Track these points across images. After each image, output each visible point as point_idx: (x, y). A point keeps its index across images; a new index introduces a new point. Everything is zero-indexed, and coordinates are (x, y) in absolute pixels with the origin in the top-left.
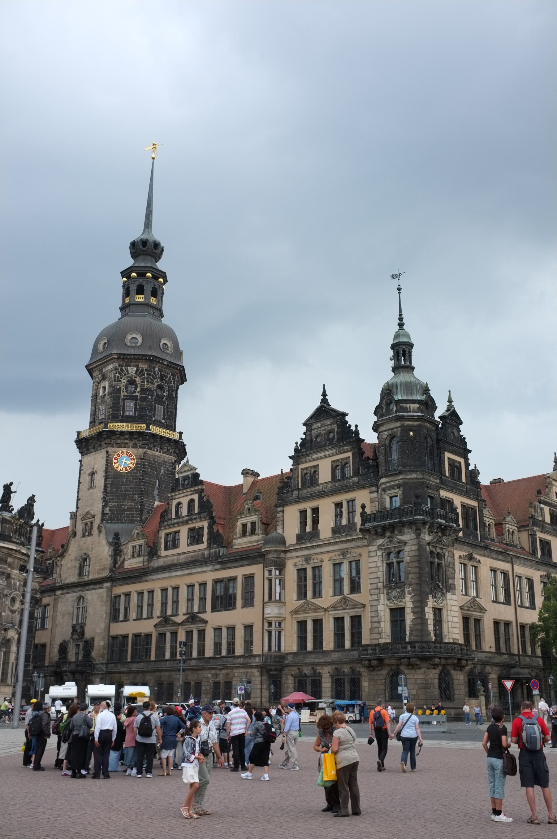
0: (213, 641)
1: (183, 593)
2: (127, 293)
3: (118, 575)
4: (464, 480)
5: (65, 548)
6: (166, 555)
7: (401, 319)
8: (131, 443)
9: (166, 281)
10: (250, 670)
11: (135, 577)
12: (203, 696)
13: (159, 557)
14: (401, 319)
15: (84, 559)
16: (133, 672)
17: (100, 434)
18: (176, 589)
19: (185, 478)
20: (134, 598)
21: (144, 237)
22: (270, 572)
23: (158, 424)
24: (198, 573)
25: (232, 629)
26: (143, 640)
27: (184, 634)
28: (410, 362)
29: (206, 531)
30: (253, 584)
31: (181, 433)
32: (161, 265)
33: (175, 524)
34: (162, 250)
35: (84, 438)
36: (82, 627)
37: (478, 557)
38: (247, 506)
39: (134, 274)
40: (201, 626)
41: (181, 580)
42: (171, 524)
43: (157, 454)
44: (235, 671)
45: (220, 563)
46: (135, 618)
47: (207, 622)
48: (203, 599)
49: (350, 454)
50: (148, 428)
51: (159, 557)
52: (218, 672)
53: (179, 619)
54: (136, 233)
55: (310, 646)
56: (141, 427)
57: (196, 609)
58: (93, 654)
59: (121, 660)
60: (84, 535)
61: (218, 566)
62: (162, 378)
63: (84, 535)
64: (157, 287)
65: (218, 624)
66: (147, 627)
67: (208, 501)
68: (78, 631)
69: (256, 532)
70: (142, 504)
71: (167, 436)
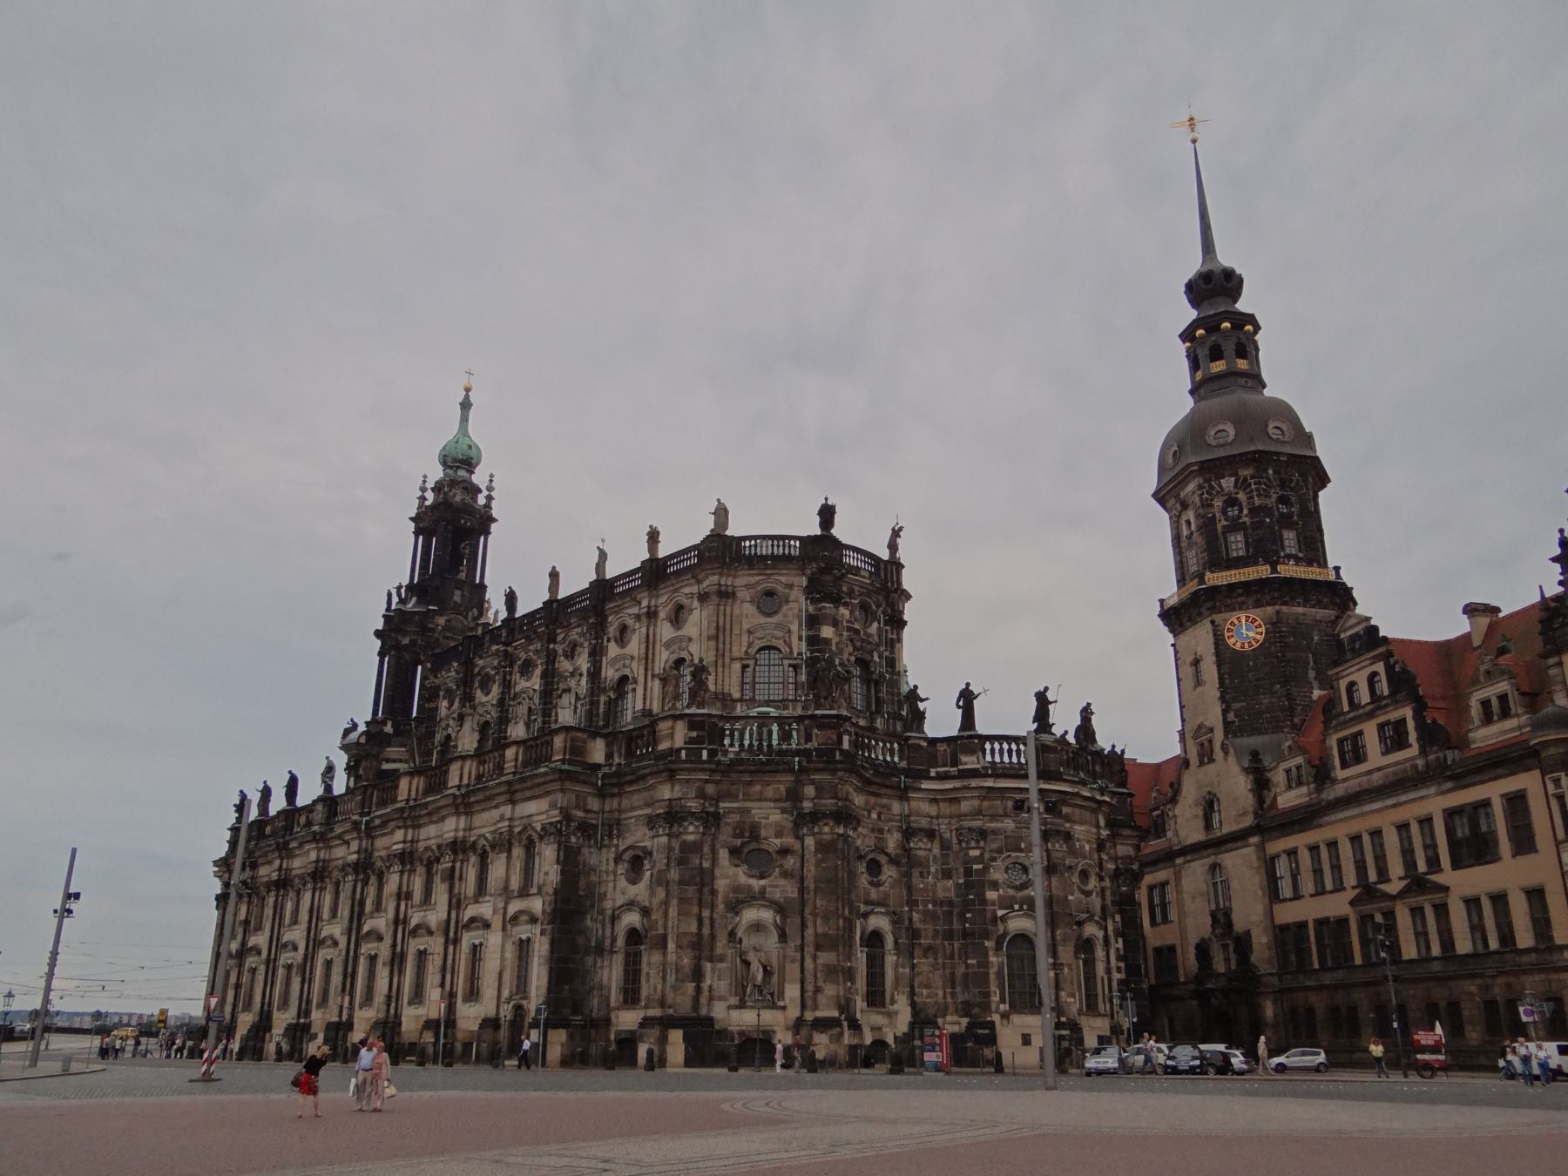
0: (1467, 924)
1: (1392, 841)
2: (1195, 365)
3: (1270, 823)
5: (1176, 787)
6: (1347, 778)
8: (1251, 601)
9: (1257, 328)
10: (1555, 976)
11: (1299, 821)
12: (1468, 1028)
13: (1334, 781)
15: (1209, 805)
16: (1327, 987)
17: (1195, 594)
18: (1376, 834)
19: (1353, 638)
20: (1305, 858)
21: (1205, 269)
22: (1557, 782)
24: (1413, 800)
25: (1500, 900)
26: (1333, 928)
27: (1407, 911)
29: (1411, 725)
30: (1526, 810)
31: (1337, 569)
32: (1242, 305)
33: (1351, 720)
34: (1241, 281)
35: (1172, 608)
36: (1227, 913)
38: (1483, 668)
39: (1200, 332)
40: (1437, 897)
41: (1384, 816)
42: (1345, 722)
43: (1301, 610)
44: (1527, 980)
45: (1450, 778)
46: (1312, 891)
47: (1446, 889)
50: (1274, 570)
51: (1334, 781)
52: (1489, 981)
53: (1394, 887)
54: (1193, 264)
56: (1262, 571)
57: (1422, 867)
58: (1253, 959)
59: (1303, 967)
60: (1202, 763)
61: (1449, 785)
62: (1283, 485)
63: (1202, 763)
64: (1244, 340)
65: (1469, 892)
66: (1337, 905)
67: (1404, 671)
68: (1222, 919)
69: (1513, 711)
70: (1289, 697)
71: (1311, 577)
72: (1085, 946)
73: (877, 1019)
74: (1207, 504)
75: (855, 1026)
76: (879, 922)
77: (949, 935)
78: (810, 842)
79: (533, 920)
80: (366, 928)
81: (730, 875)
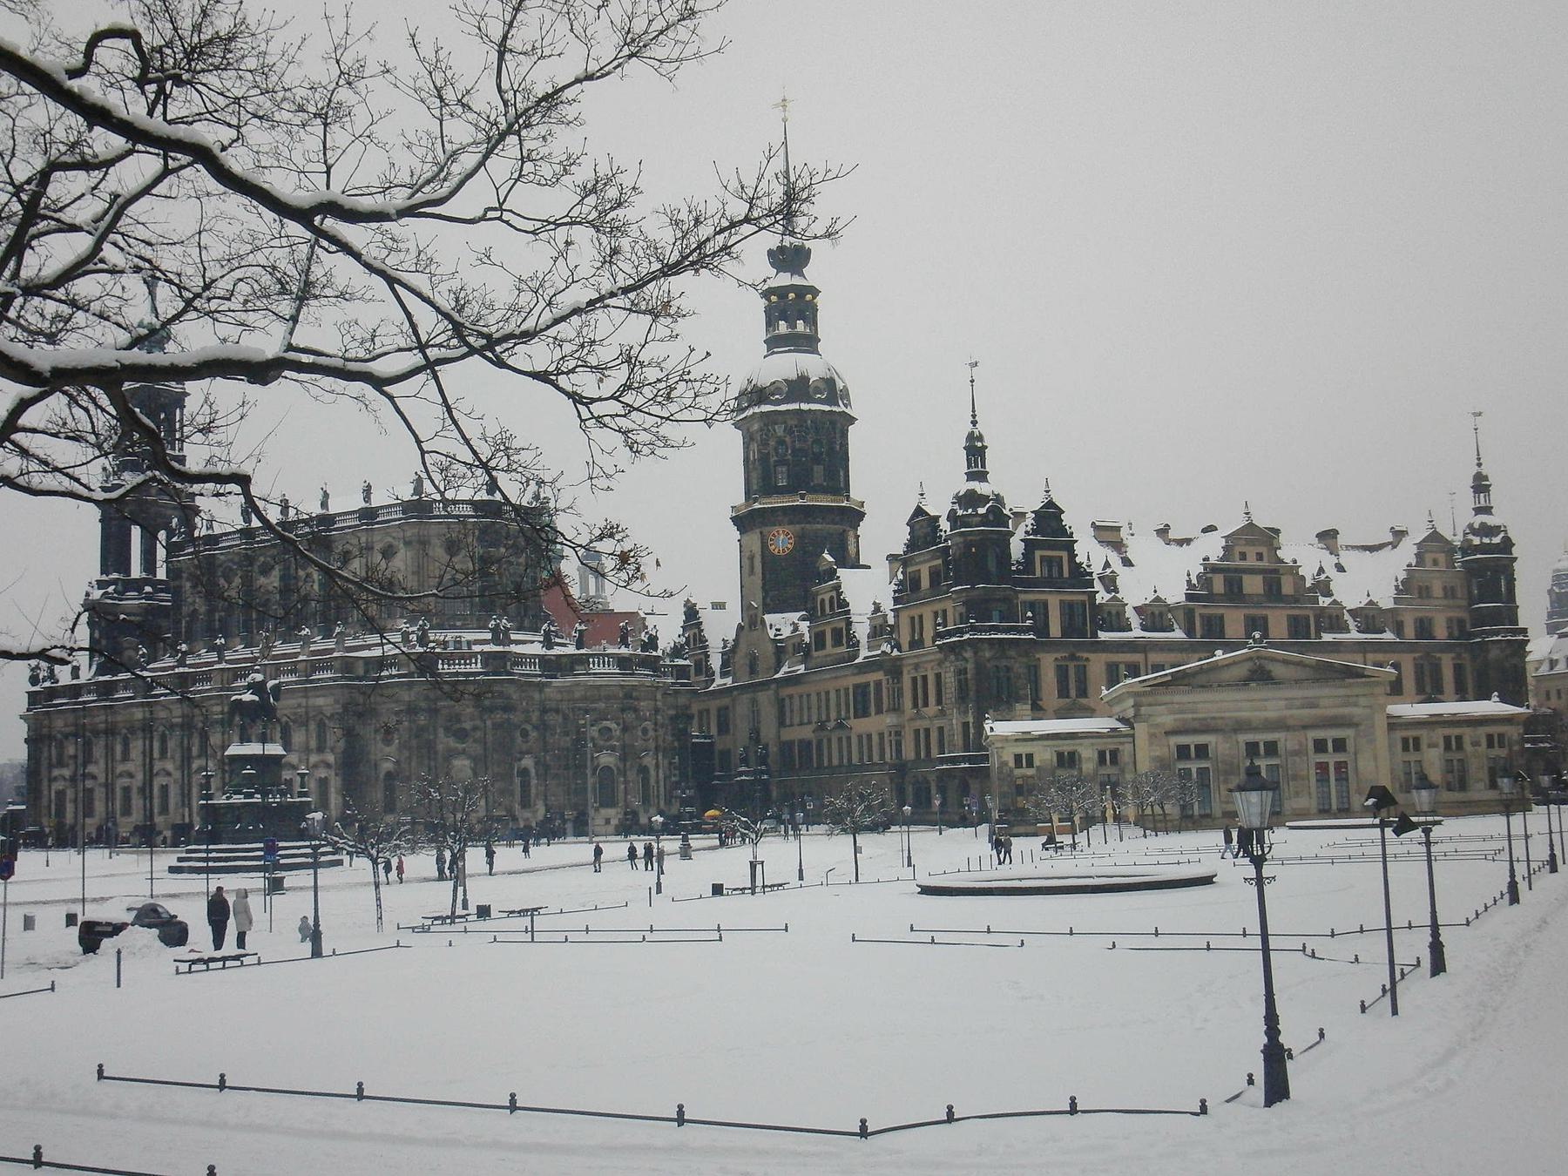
1: (833, 696)
2: (770, 323)
4: (1066, 574)
7: (974, 416)
14: (974, 416)
18: (827, 693)
23: (815, 490)
26: (805, 745)
28: (983, 466)
36: (758, 733)
37: (1085, 655)
39: (774, 298)
48: (847, 705)
49: (939, 561)
53: (831, 725)
55: (923, 755)
66: (807, 733)
72: (644, 770)
73: (527, 814)
74: (764, 443)
75: (515, 819)
76: (528, 762)
77: (567, 768)
78: (489, 723)
79: (328, 766)
80: (195, 766)
81: (444, 741)
